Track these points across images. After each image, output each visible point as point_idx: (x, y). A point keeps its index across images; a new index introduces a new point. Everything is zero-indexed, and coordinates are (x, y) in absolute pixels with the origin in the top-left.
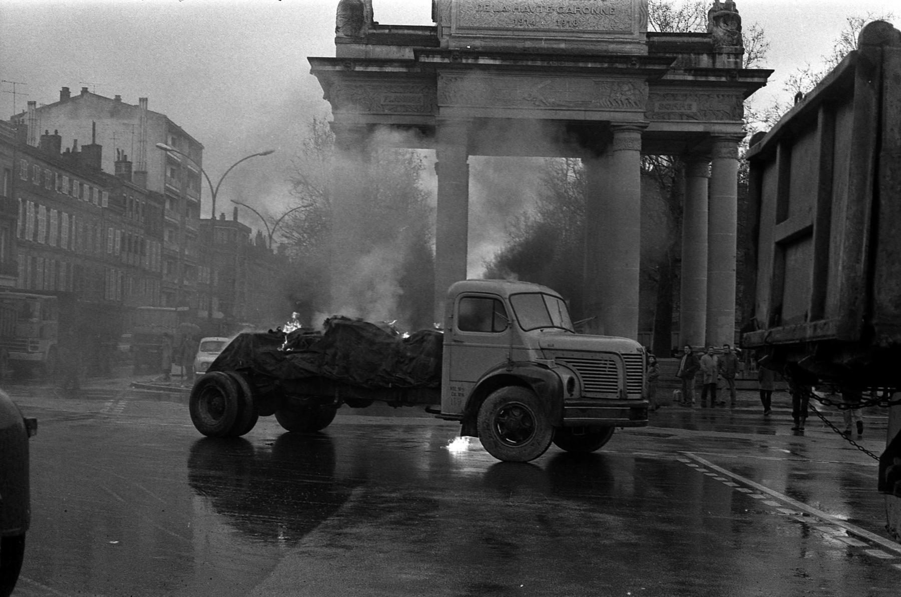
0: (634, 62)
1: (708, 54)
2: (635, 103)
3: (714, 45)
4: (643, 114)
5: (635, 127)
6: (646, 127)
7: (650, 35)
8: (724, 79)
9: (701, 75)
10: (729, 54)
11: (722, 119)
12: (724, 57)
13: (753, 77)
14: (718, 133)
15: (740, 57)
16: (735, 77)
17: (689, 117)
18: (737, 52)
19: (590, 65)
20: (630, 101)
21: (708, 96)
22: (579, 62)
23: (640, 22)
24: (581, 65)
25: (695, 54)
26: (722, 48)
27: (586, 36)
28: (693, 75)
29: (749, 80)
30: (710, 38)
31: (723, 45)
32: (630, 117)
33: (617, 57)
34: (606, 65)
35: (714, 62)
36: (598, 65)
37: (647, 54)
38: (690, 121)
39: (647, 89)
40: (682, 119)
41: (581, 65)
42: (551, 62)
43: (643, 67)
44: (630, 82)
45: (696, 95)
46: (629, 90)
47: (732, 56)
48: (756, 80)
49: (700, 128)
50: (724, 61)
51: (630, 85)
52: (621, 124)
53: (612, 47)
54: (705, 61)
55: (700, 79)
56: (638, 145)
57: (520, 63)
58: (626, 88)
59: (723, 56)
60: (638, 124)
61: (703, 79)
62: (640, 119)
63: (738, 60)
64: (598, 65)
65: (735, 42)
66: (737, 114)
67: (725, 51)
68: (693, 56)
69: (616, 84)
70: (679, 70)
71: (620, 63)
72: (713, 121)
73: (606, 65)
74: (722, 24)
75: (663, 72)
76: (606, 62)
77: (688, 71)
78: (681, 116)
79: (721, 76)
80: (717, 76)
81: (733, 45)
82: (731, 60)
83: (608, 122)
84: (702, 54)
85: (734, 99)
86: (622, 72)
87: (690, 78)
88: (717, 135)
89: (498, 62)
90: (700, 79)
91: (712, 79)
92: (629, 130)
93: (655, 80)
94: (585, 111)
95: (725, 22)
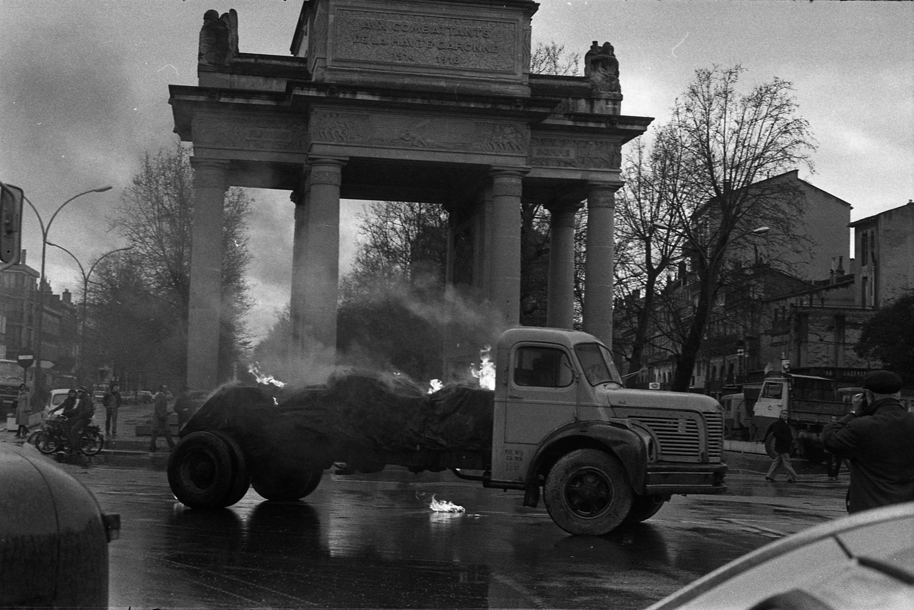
2: (517, 146)
3: (593, 89)
7: (532, 76)
8: (603, 126)
13: (633, 124)
16: (615, 124)
17: (567, 164)
23: (523, 61)
25: (573, 98)
27: (467, 74)
28: (572, 120)
30: (588, 82)
34: (489, 106)
35: (592, 107)
40: (560, 166)
43: (527, 110)
46: (512, 133)
50: (601, 108)
53: (495, 88)
54: (583, 106)
58: (508, 130)
60: (521, 170)
65: (613, 87)
68: (571, 100)
73: (489, 106)
74: (600, 69)
75: (545, 116)
77: (568, 116)
78: (559, 162)
83: (488, 167)
87: (570, 123)
95: (603, 67)
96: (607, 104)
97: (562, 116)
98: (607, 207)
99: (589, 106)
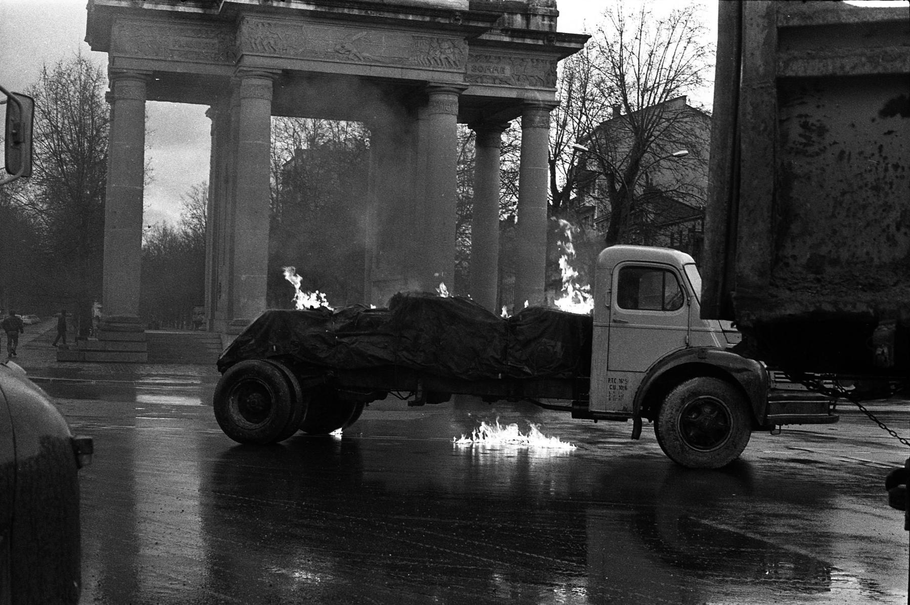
0: (458, 17)
1: (522, 15)
2: (454, 62)
3: (528, 4)
4: (462, 75)
5: (452, 89)
6: (463, 90)
8: (540, 42)
9: (518, 37)
10: (543, 16)
11: (535, 85)
12: (539, 19)
14: (532, 100)
15: (554, 19)
18: (552, 14)
19: (411, 18)
20: (450, 60)
21: (522, 60)
22: (400, 13)
24: (401, 17)
25: (509, 13)
26: (537, 9)
29: (566, 45)
31: (537, 5)
32: (447, 78)
33: (440, 10)
34: (427, 19)
35: (528, 24)
36: (419, 18)
37: (467, 9)
38: (503, 86)
39: (468, 47)
41: (401, 17)
42: (369, 12)
44: (450, 39)
45: (510, 58)
46: (449, 48)
47: (546, 19)
48: (573, 45)
49: (513, 94)
50: (538, 24)
51: (451, 43)
52: (439, 85)
54: (518, 21)
55: (516, 41)
56: (455, 109)
57: (335, 11)
58: (446, 45)
59: (537, 17)
60: (458, 87)
61: (520, 41)
62: (459, 80)
63: (553, 23)
64: (419, 18)
66: (550, 80)
67: (540, 12)
69: (435, 41)
70: (496, 29)
71: (442, 17)
72: (526, 88)
73: (427, 19)
76: (427, 16)
79: (538, 39)
80: (534, 39)
81: (548, 7)
82: (545, 22)
84: (516, 14)
85: (548, 65)
86: (442, 28)
87: (507, 39)
88: (530, 102)
89: (311, 8)
90: (516, 41)
91: (529, 41)
92: (448, 92)
93: (473, 38)
94: (402, 68)
96: (543, 20)
97: (498, 32)
98: (542, 127)
99: (525, 22)
